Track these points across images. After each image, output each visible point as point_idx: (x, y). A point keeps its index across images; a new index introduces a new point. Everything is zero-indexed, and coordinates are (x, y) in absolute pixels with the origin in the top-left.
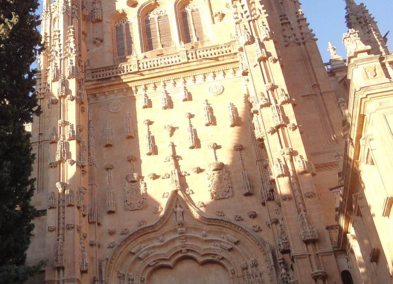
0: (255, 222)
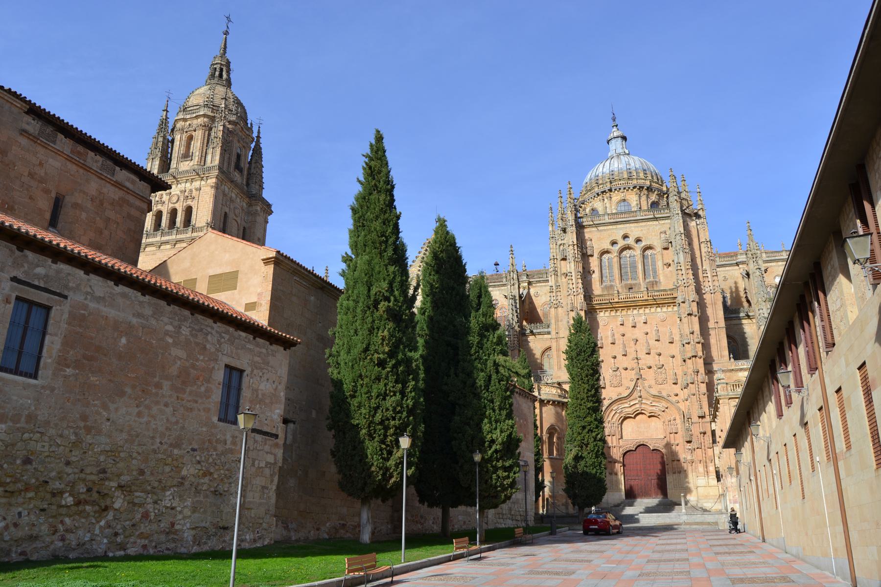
0: (677, 398)
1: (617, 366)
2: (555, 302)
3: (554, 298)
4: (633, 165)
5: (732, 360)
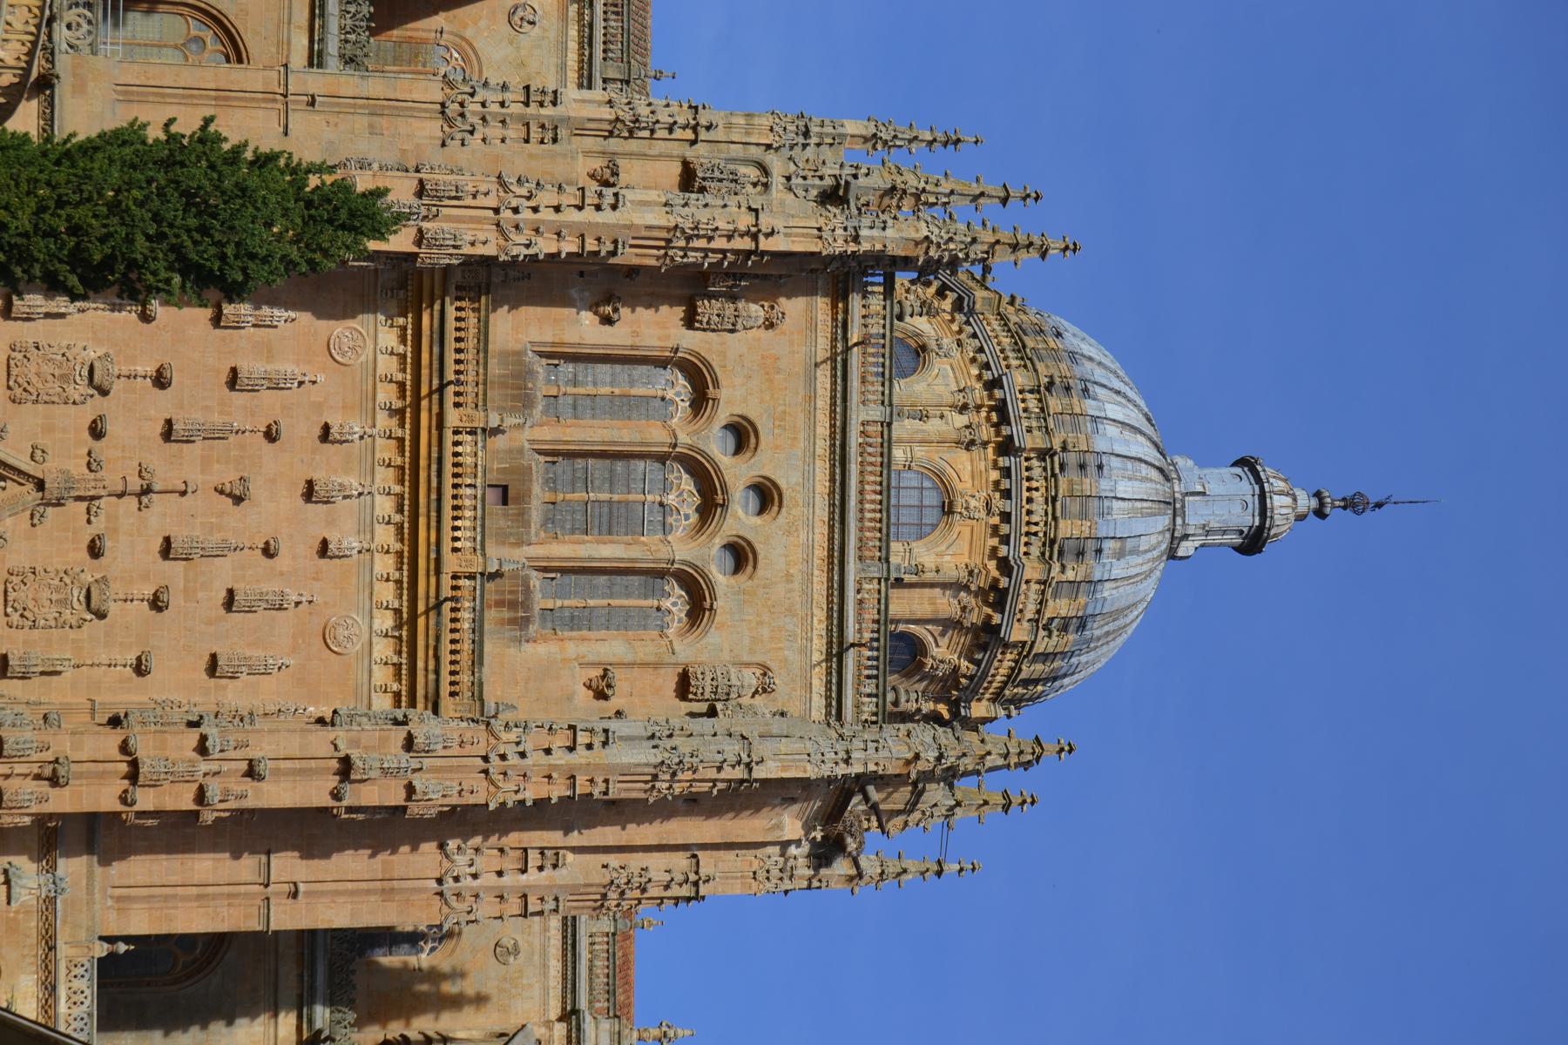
1: (117, 387)
2: (473, 107)
3: (495, 108)
4: (1116, 573)
5: (102, 950)
